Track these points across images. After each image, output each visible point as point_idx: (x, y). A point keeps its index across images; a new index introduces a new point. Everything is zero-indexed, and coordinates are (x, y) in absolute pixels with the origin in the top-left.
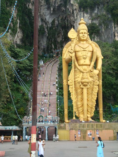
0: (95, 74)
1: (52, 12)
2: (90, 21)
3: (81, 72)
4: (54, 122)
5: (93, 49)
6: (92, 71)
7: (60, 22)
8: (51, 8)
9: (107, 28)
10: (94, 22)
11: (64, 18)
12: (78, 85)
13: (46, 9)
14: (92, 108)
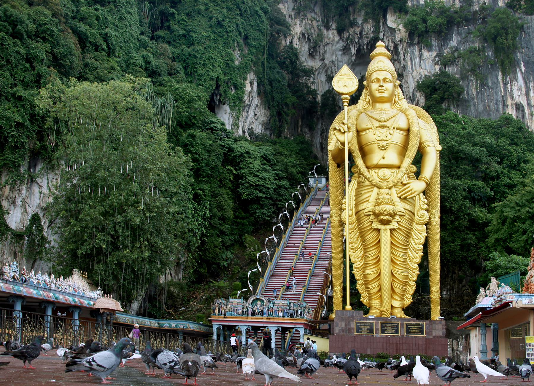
0: (415, 192)
1: (354, 58)
2: (437, 68)
3: (374, 185)
4: (291, 316)
6: (405, 182)
9: (483, 84)
10: (449, 70)
12: (366, 223)
13: (340, 53)
14: (405, 284)
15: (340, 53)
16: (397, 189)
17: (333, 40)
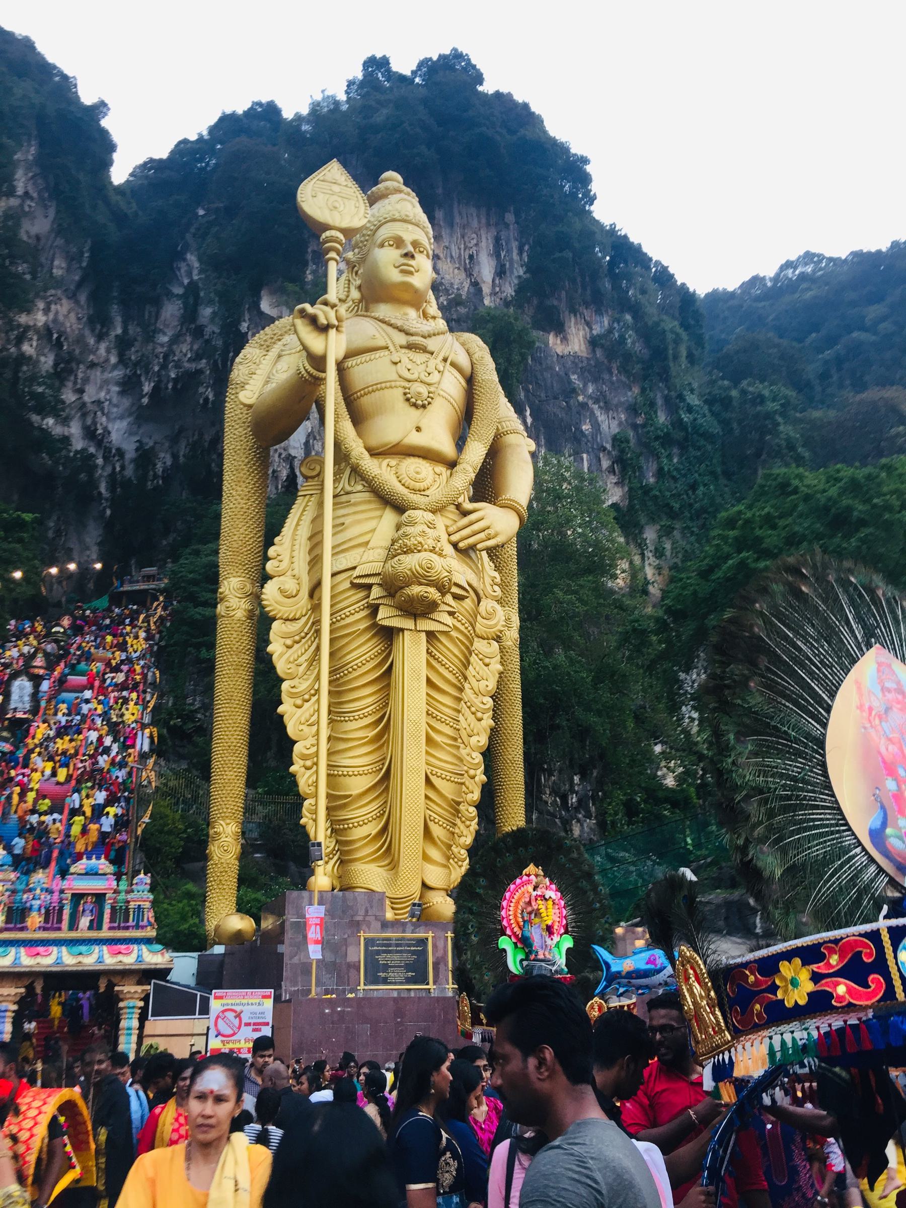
1: (145, 401)
5: (472, 364)
6: (468, 506)
7: (182, 460)
8: (140, 384)
11: (206, 444)
13: (116, 389)
15: (116, 389)
16: (449, 522)
17: (107, 360)
